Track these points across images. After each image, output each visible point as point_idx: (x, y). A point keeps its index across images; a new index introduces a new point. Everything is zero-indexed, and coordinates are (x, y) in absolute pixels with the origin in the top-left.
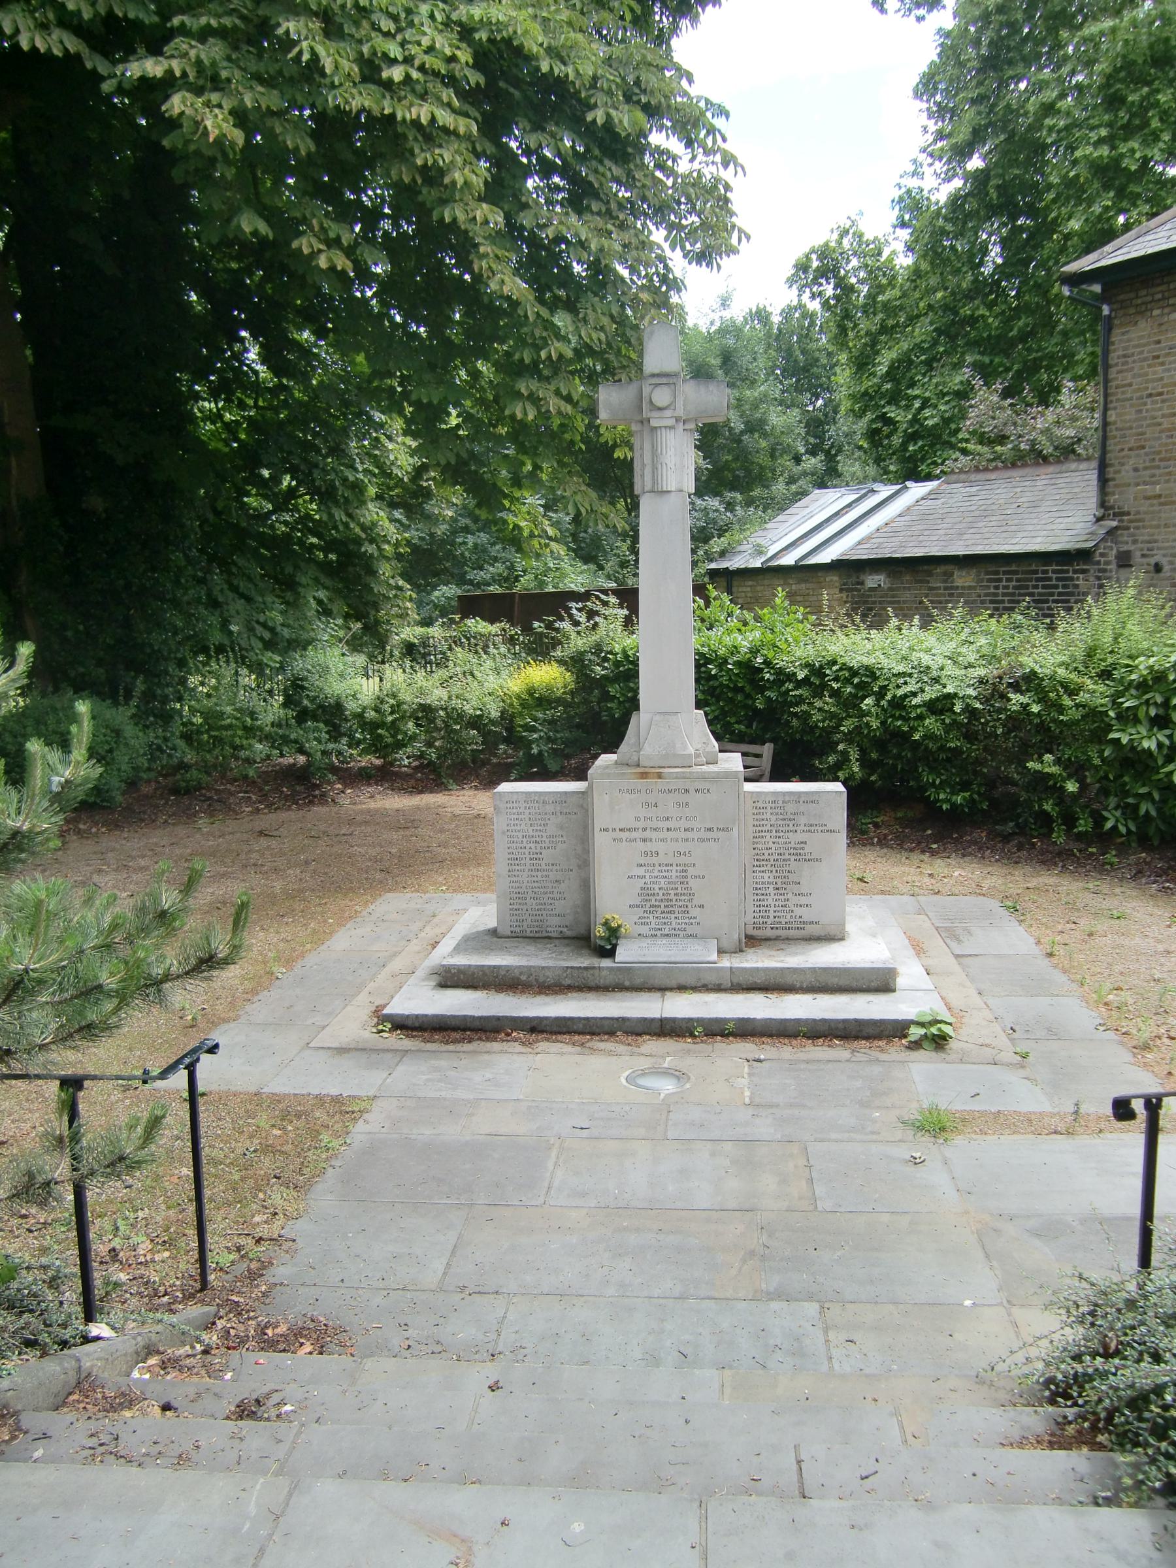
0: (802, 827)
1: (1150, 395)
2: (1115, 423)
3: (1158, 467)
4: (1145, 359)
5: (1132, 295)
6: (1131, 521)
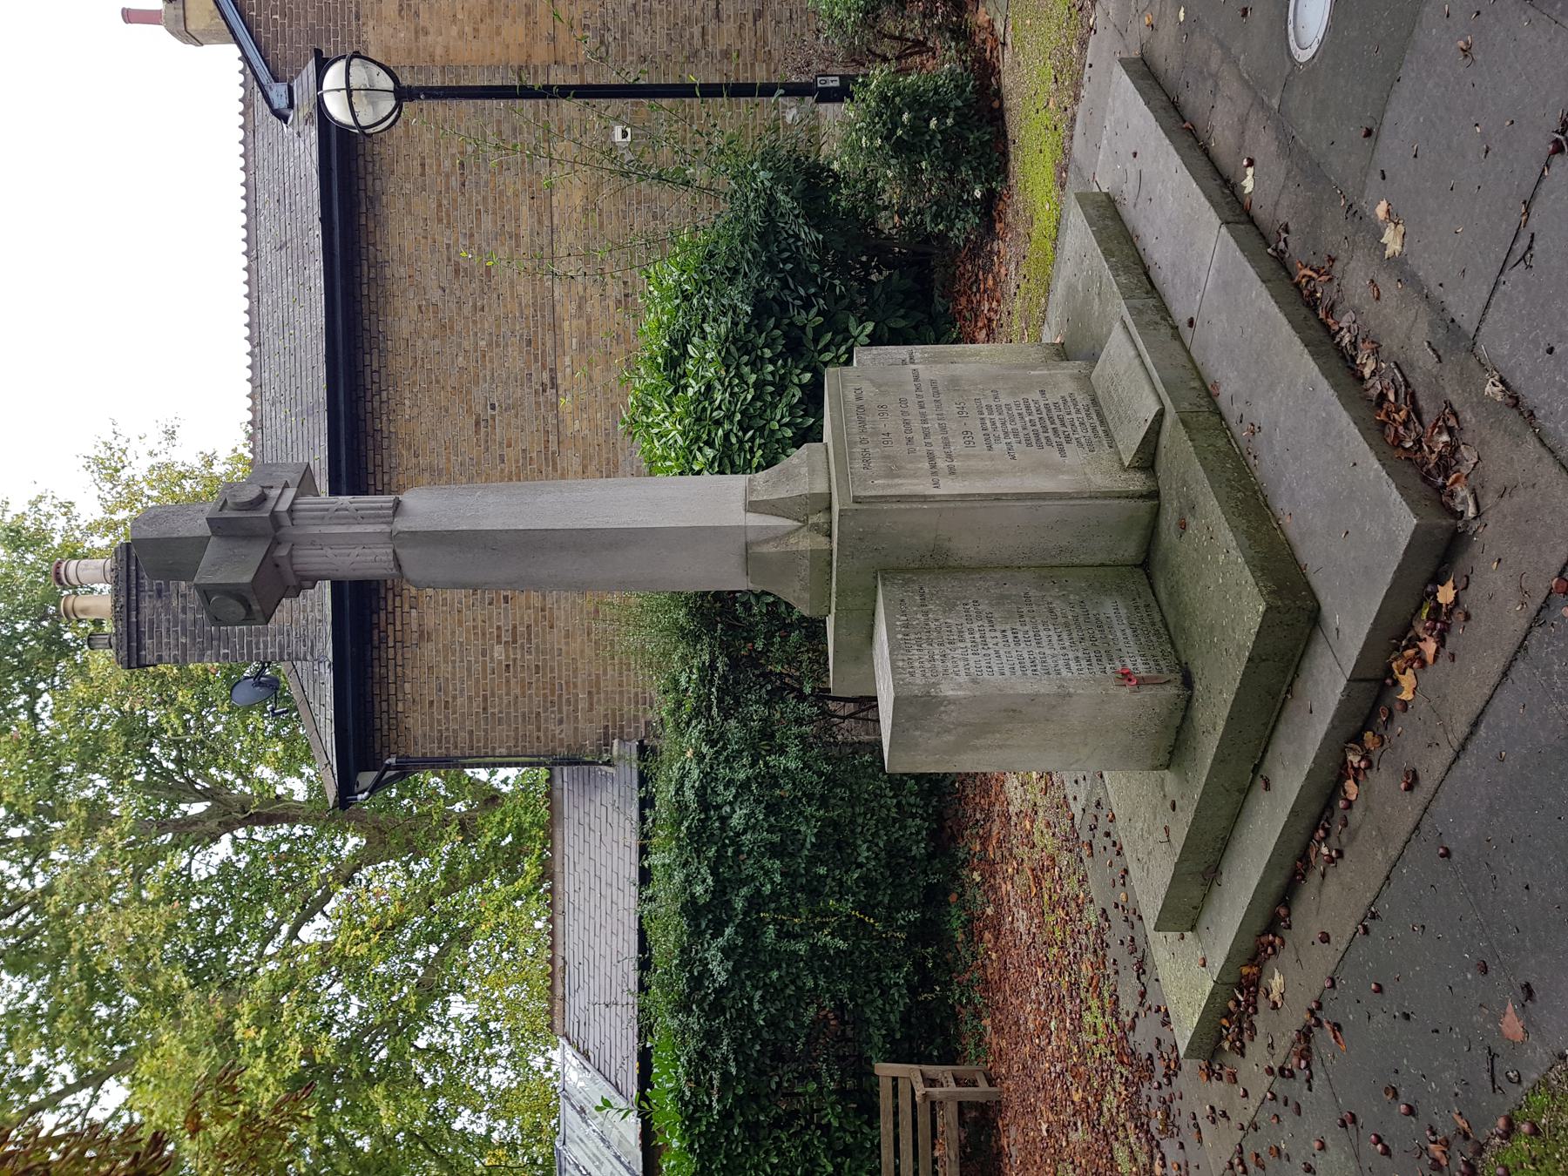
1: (485, 709)
2: (509, 748)
3: (560, 696)
4: (447, 718)
5: (378, 734)
6: (614, 727)
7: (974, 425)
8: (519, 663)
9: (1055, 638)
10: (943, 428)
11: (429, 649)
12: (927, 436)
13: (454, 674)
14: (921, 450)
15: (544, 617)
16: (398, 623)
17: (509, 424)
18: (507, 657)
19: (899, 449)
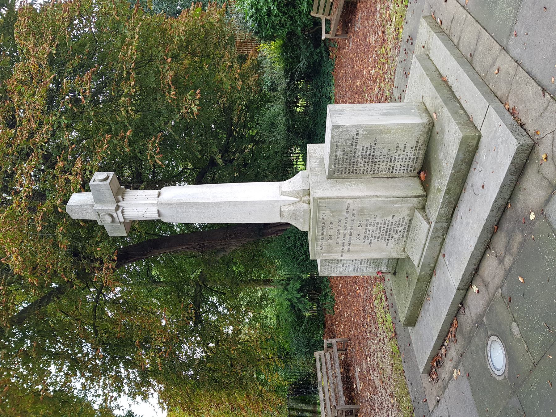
0: (353, 149)
7: (362, 232)
10: (351, 233)
12: (344, 236)
14: (341, 242)
19: (333, 242)
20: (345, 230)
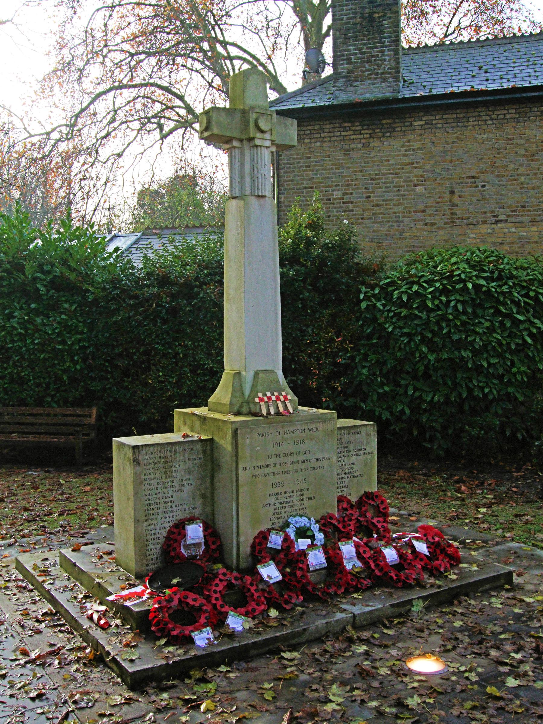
0: (352, 453)
1: (305, 188)
2: (284, 202)
4: (301, 167)
8: (331, 206)
9: (168, 520)
10: (287, 472)
11: (340, 155)
12: (282, 464)
13: (326, 170)
15: (358, 219)
16: (354, 137)
17: (473, 196)
18: (334, 199)
20: (292, 463)
